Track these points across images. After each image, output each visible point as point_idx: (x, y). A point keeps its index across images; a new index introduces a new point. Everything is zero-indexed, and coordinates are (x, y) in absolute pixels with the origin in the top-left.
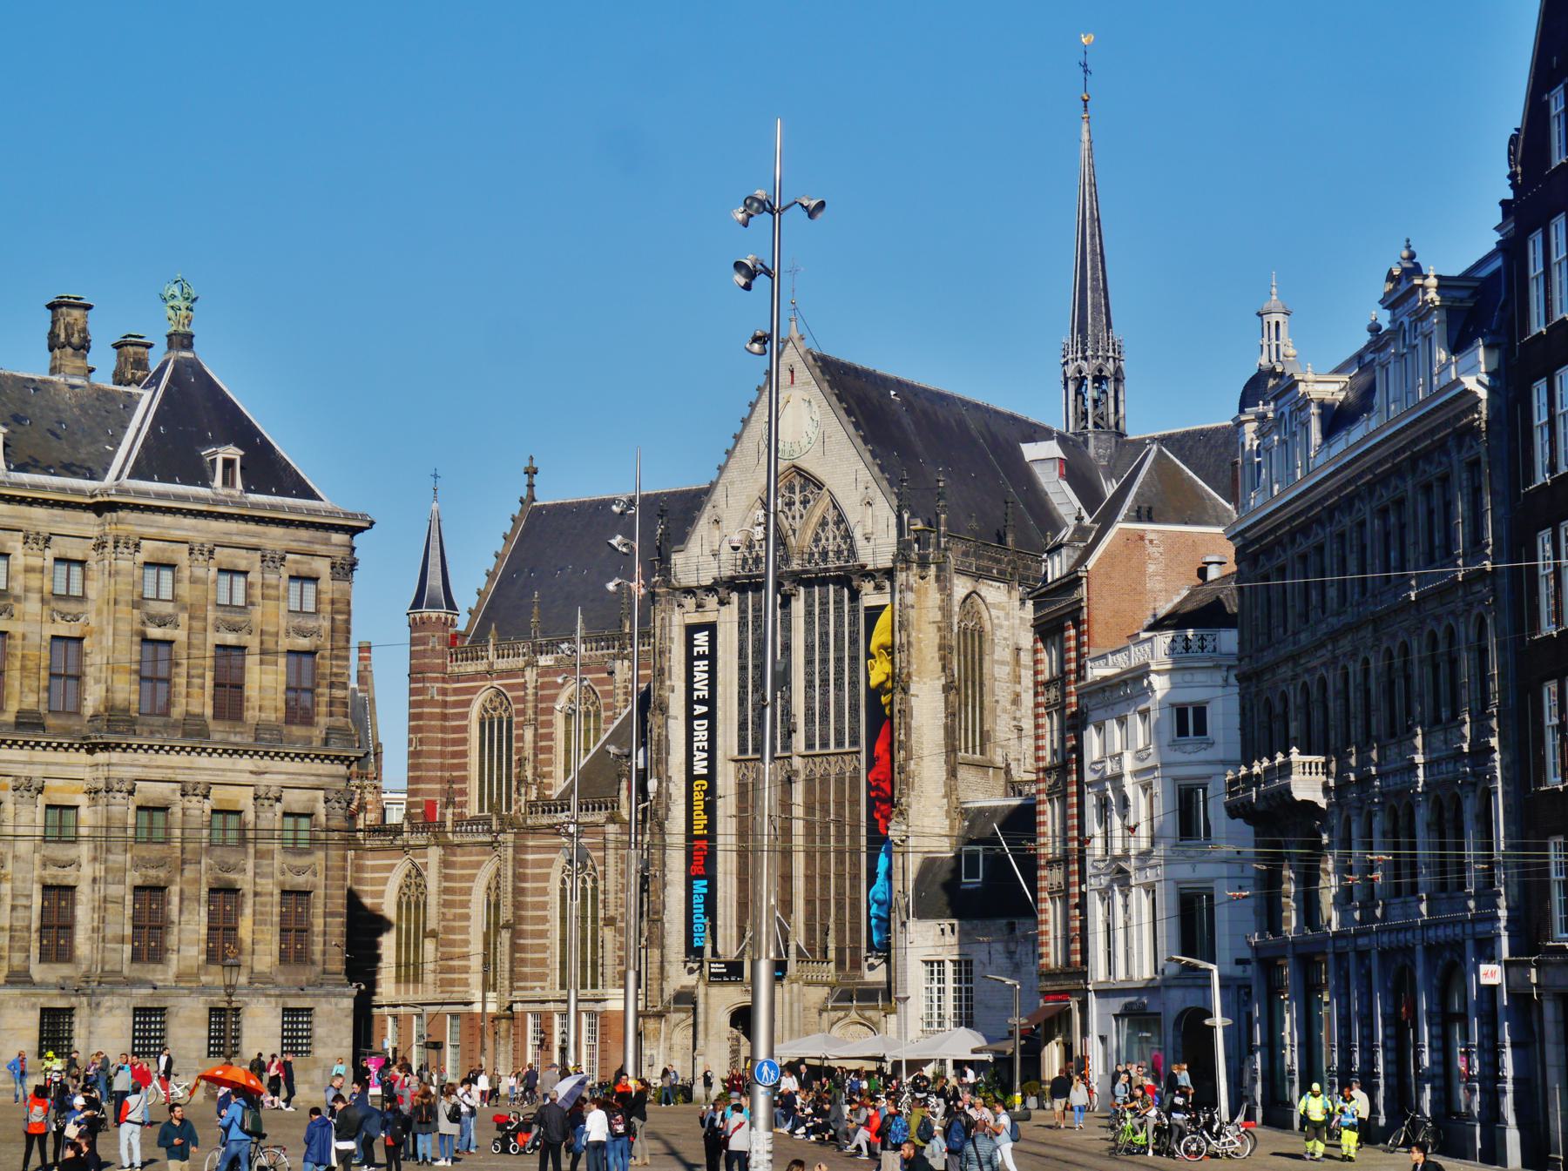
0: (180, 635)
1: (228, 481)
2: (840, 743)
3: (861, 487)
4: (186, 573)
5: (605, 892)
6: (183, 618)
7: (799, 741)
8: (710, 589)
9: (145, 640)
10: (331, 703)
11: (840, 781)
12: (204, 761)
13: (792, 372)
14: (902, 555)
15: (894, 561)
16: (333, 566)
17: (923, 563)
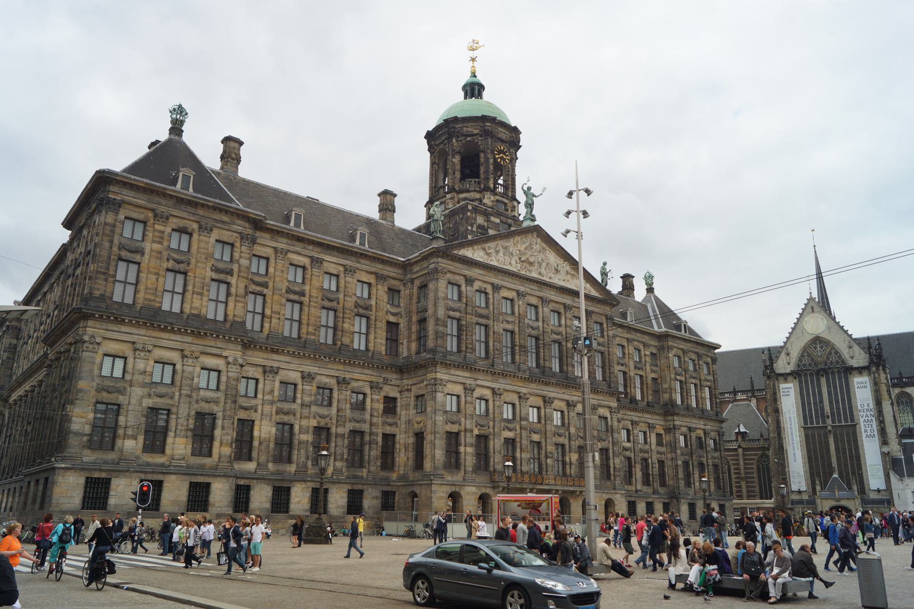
0: (683, 379)
1: (685, 332)
2: (846, 421)
3: (847, 342)
4: (682, 359)
5: (738, 469)
6: (683, 373)
7: (829, 421)
8: (788, 374)
9: (676, 380)
10: (716, 404)
11: (848, 434)
12: (694, 421)
13: (813, 308)
14: (871, 362)
15: (870, 364)
16: (712, 360)
17: (877, 366)
